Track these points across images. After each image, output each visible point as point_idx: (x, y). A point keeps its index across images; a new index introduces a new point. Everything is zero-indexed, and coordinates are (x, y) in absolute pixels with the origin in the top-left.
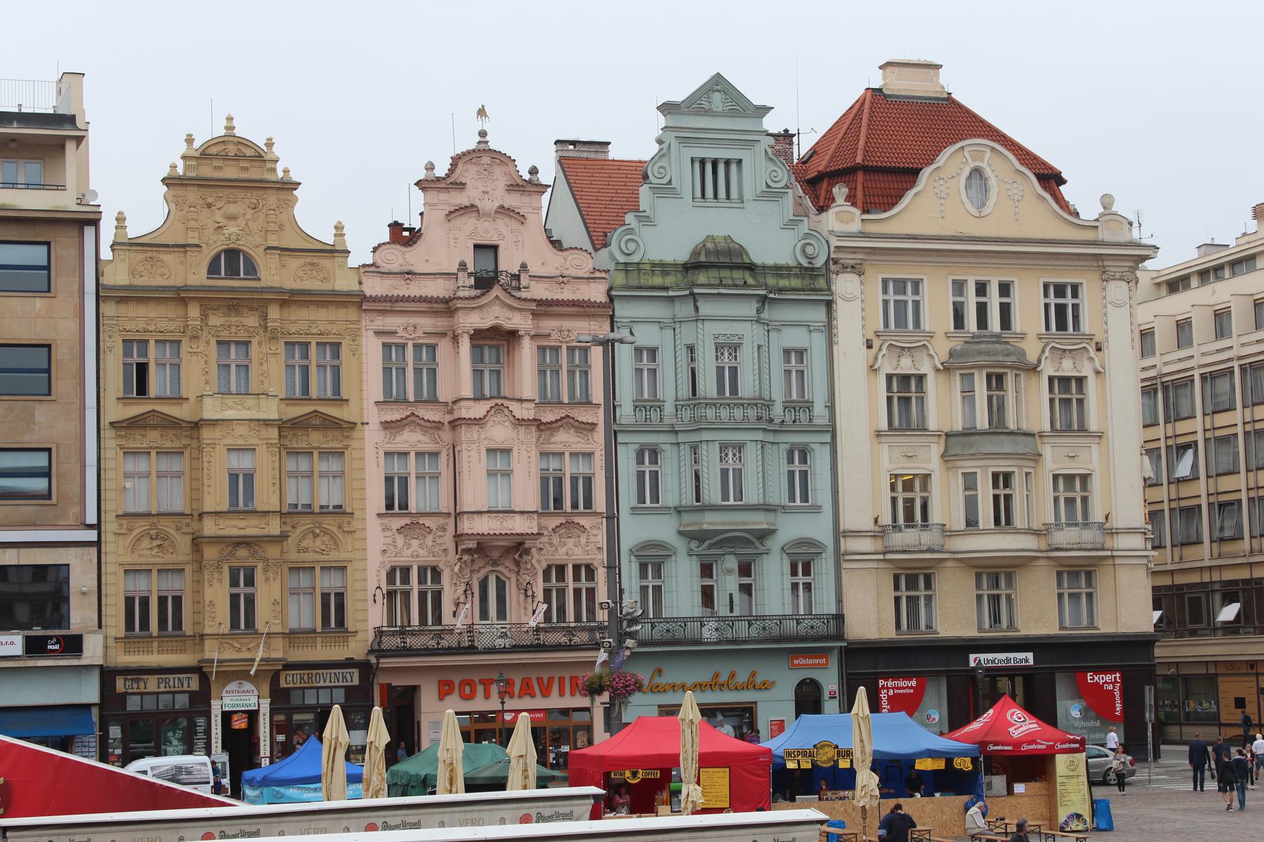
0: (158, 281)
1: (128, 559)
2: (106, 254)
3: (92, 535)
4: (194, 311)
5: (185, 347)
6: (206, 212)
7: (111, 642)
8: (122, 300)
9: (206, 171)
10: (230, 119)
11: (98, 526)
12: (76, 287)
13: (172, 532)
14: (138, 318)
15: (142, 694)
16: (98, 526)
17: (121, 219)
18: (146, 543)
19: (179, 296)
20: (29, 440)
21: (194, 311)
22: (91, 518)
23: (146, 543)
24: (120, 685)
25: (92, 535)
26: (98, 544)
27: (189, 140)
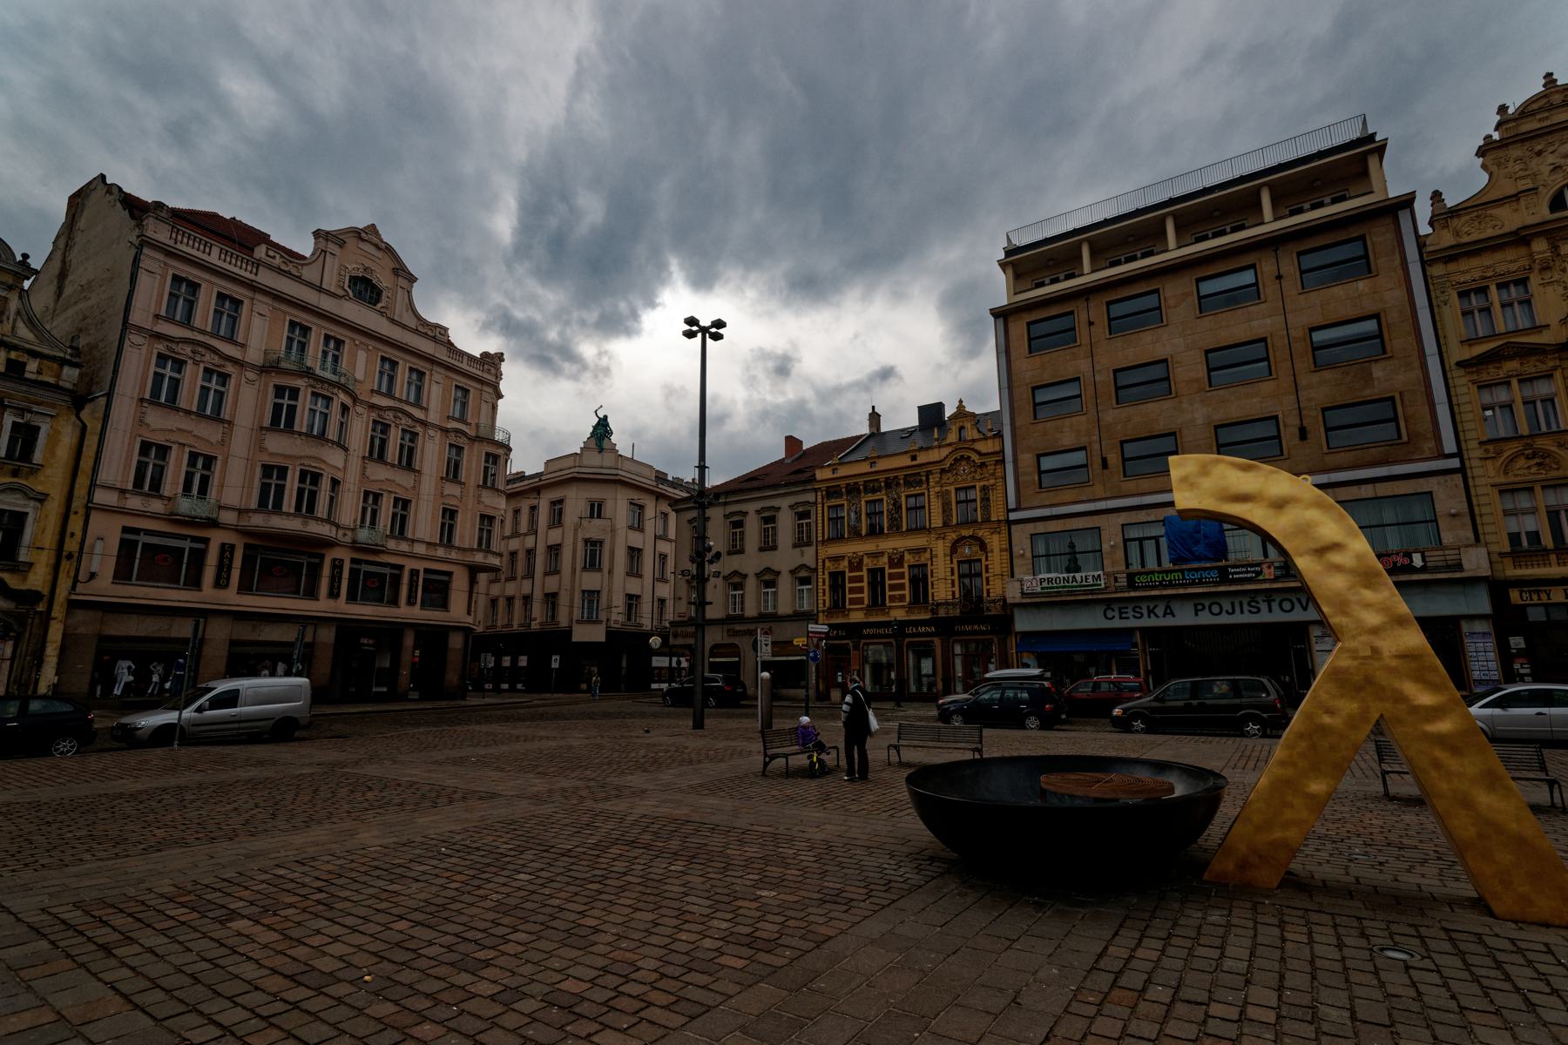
0: (1490, 233)
1: (1502, 479)
2: (1425, 229)
3: (1455, 463)
4: (1540, 246)
5: (1535, 280)
6: (1536, 160)
7: (1496, 558)
8: (1449, 259)
9: (1529, 126)
10: (1549, 75)
11: (1459, 454)
12: (1397, 262)
13: (1554, 449)
14: (1469, 271)
15: (1546, 606)
16: (1459, 454)
17: (1437, 196)
18: (1521, 462)
19: (1521, 238)
20: (1368, 393)
21: (1540, 246)
22: (1450, 446)
23: (1521, 462)
24: (1515, 596)
25: (1455, 463)
26: (1462, 470)
27: (1503, 109)
